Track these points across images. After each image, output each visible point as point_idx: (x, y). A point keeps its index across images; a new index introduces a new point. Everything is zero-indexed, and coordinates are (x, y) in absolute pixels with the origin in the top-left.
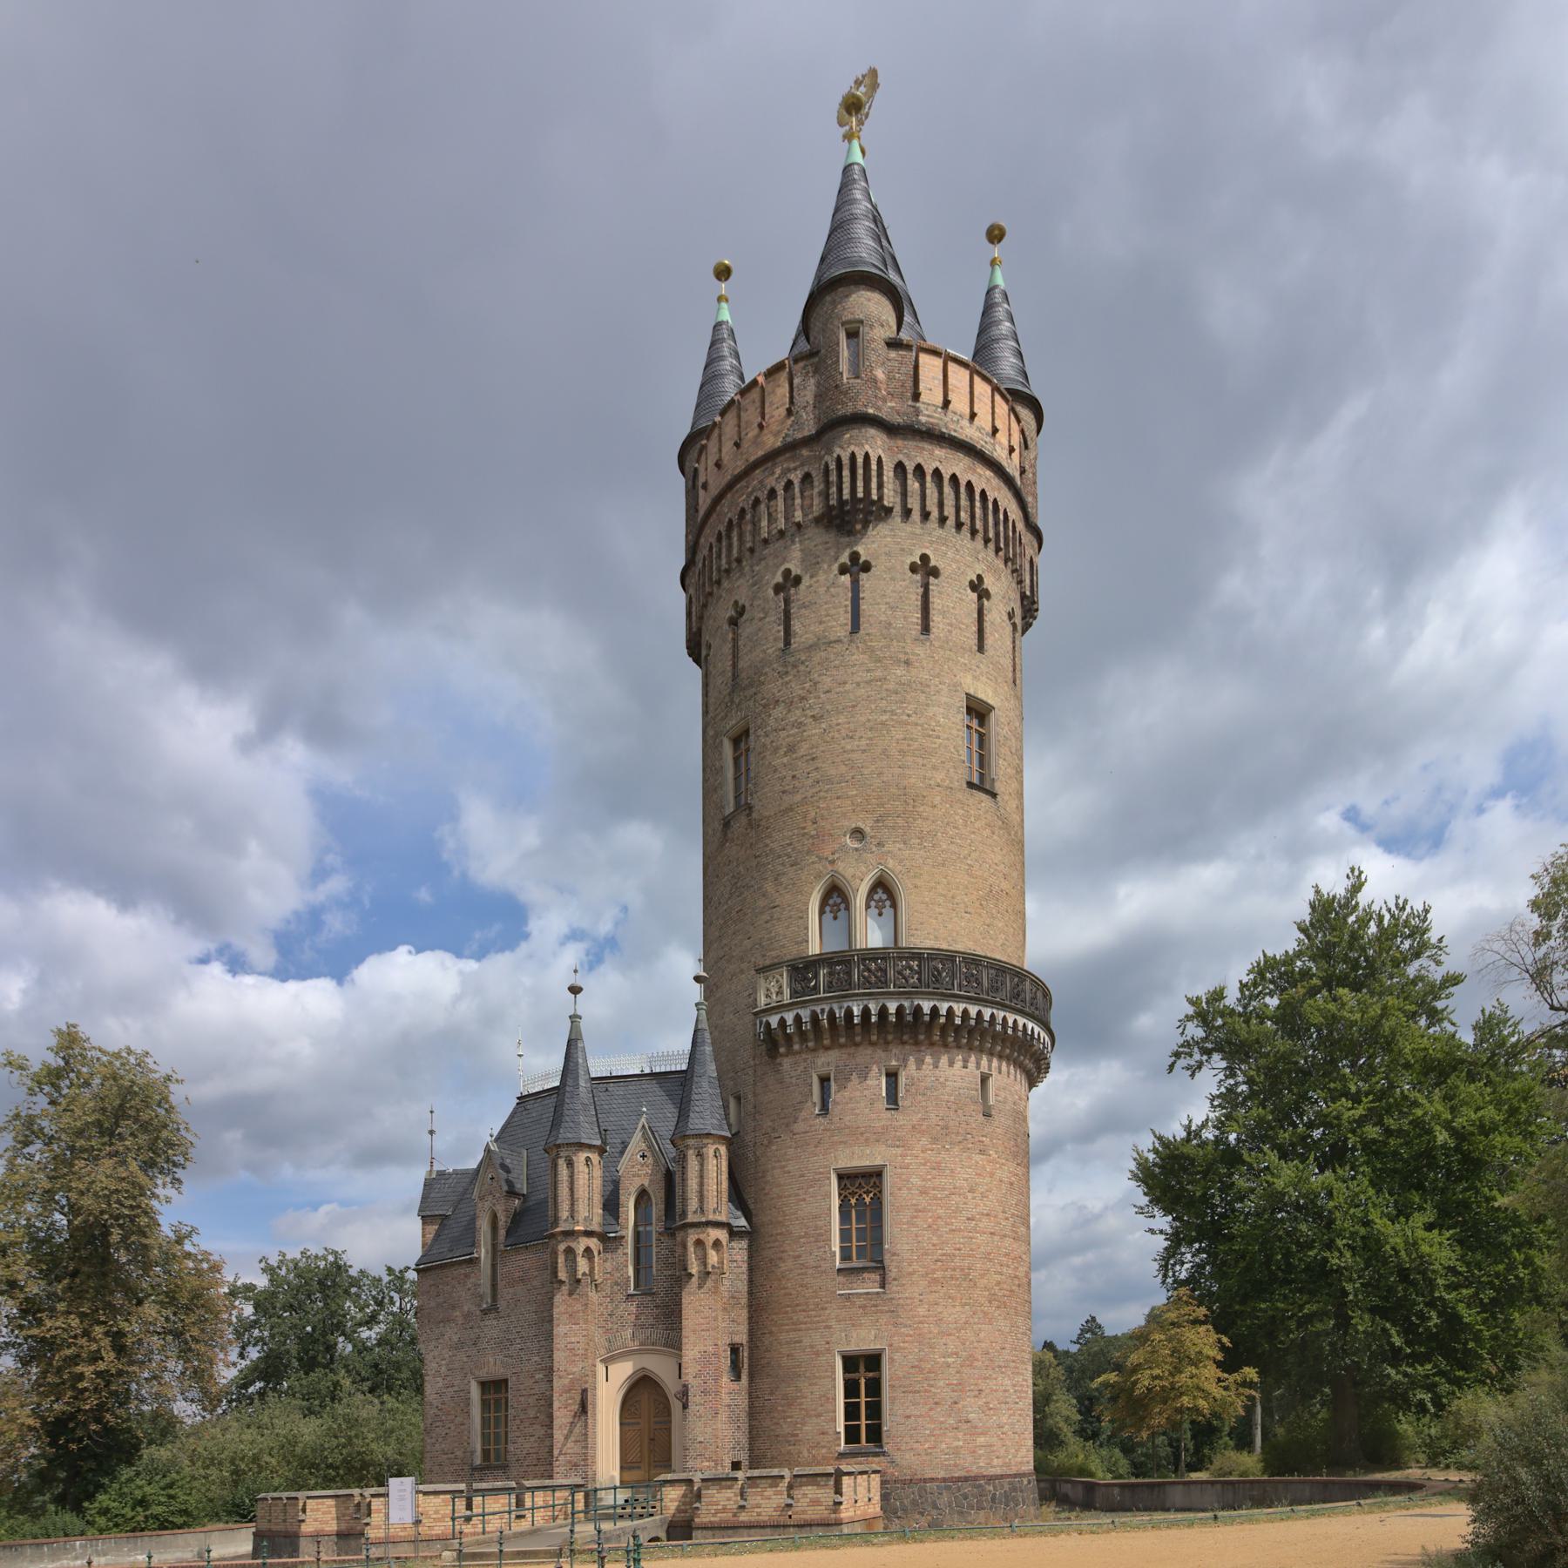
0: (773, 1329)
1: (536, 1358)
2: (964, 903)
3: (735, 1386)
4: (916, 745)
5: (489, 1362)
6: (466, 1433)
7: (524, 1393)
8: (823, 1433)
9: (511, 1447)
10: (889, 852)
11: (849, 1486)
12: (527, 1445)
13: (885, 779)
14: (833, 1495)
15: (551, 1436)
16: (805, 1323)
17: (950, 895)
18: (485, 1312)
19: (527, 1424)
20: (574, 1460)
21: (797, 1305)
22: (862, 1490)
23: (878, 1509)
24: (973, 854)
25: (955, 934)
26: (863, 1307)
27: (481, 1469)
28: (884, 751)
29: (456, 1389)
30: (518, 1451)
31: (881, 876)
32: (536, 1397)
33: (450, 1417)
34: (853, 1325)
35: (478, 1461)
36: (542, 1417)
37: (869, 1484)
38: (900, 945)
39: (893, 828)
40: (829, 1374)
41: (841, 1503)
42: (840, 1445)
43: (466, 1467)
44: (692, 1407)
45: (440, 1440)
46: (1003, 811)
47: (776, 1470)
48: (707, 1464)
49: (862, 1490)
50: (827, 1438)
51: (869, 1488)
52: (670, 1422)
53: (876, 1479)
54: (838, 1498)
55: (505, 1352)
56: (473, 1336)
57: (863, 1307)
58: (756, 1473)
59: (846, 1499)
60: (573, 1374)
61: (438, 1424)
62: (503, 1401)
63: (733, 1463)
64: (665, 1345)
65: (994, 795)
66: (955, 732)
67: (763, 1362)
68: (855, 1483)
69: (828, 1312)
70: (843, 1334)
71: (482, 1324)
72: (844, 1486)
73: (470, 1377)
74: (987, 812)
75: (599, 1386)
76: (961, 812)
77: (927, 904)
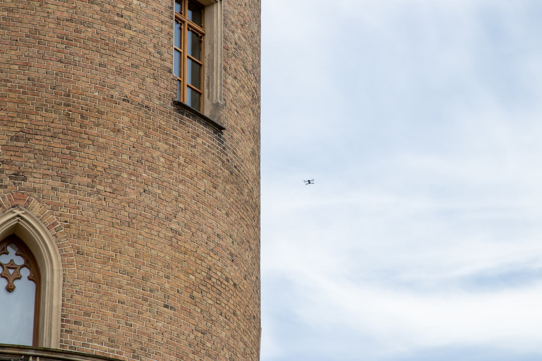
2: (164, 290)
4: (89, 33)
10: (34, 190)
13: (33, 75)
17: (139, 274)
24: (180, 215)
25: (145, 339)
28: (34, 33)
31: (17, 226)
38: (40, 346)
39: (44, 154)
46: (230, 155)
65: (218, 129)
66: (156, 24)
74: (205, 153)
76: (162, 146)
77: (98, 282)
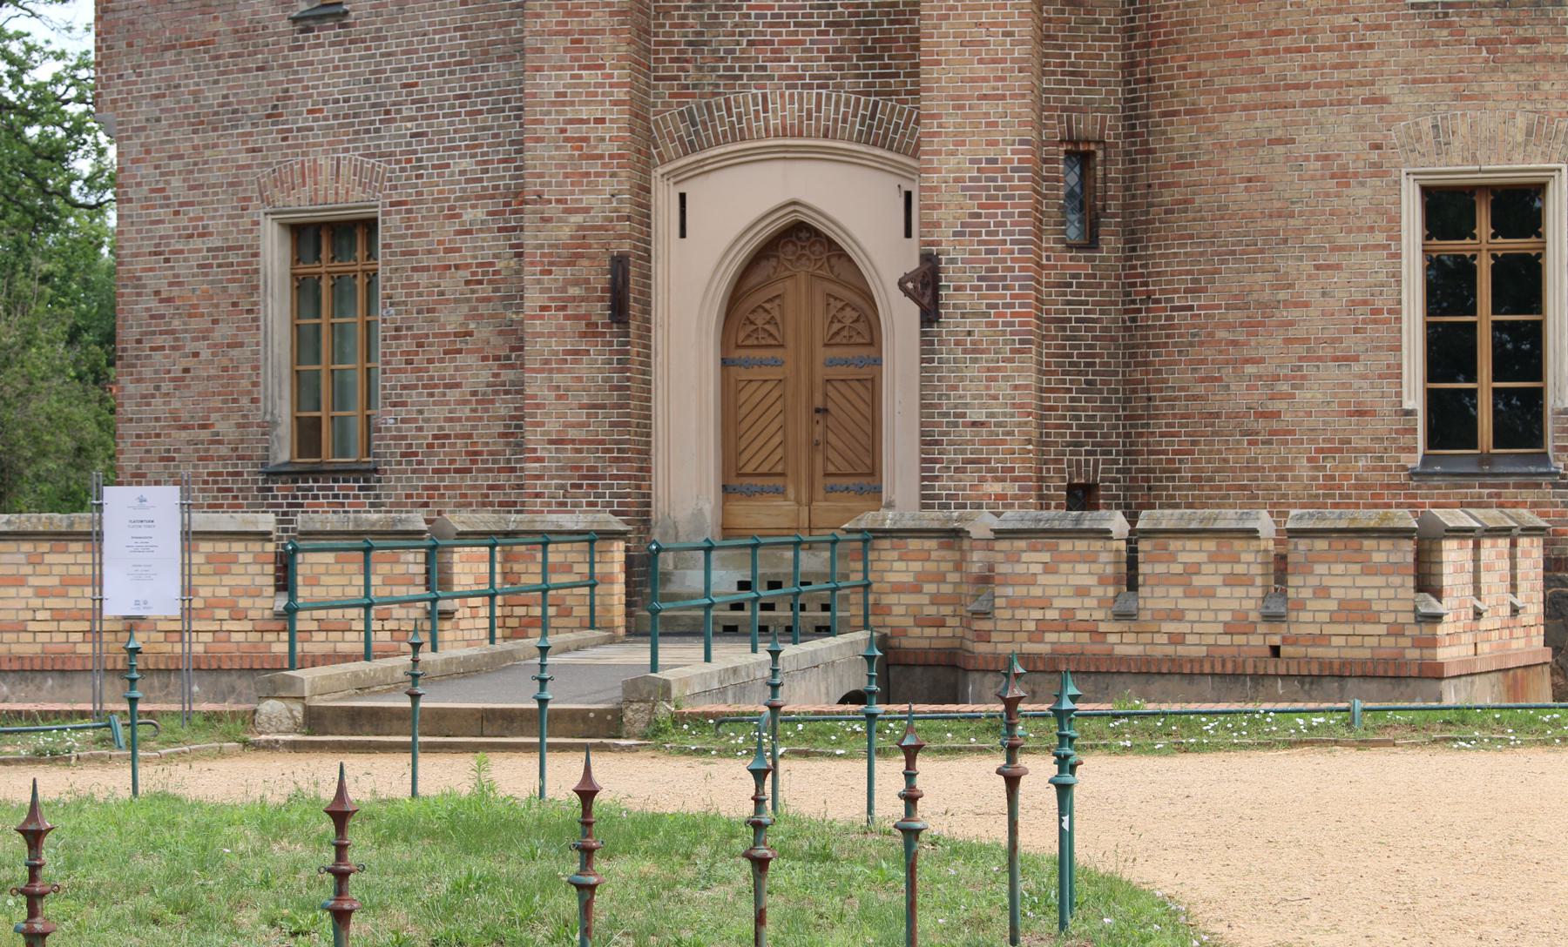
0: (1202, 101)
1: (467, 163)
3: (1079, 264)
5: (316, 170)
6: (246, 370)
7: (426, 261)
8: (1361, 413)
9: (387, 418)
11: (1460, 569)
12: (444, 412)
14: (1411, 593)
15: (518, 388)
16: (1307, 86)
18: (305, 23)
19: (436, 351)
20: (589, 459)
21: (1278, 33)
22: (1495, 583)
23: (1538, 641)
26: (1491, 43)
27: (292, 474)
29: (216, 242)
30: (409, 429)
32: (465, 274)
33: (195, 324)
34: (1459, 97)
35: (284, 452)
36: (483, 332)
37: (1513, 567)
40: (1380, 238)
41: (1437, 618)
42: (1414, 450)
43: (247, 469)
44: (951, 324)
45: (166, 387)
47: (1231, 512)
48: (996, 488)
49: (1495, 583)
50: (1380, 426)
51: (1514, 577)
52: (878, 362)
53: (1532, 554)
54: (1429, 605)
55: (368, 141)
56: (266, 92)
57: (1491, 43)
58: (1166, 518)
59: (1455, 601)
60: (587, 210)
61: (159, 340)
62: (360, 282)
63: (1071, 488)
64: (865, 137)
67: (1167, 197)
68: (1476, 560)
69: (1376, 55)
70: (1426, 124)
71: (295, 58)
72: (1447, 569)
73: (257, 210)
75: (657, 249)
